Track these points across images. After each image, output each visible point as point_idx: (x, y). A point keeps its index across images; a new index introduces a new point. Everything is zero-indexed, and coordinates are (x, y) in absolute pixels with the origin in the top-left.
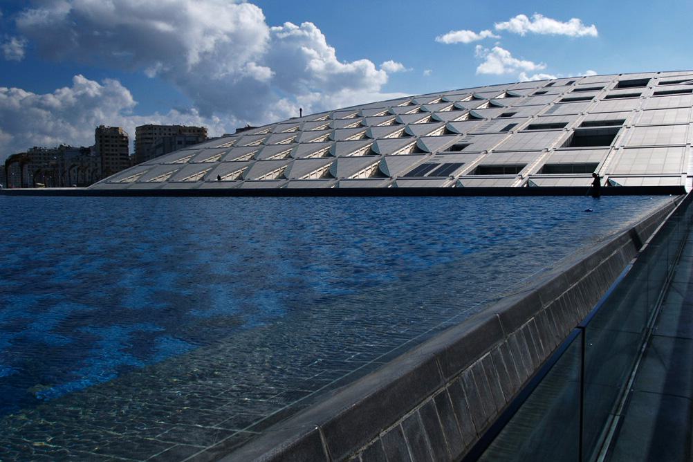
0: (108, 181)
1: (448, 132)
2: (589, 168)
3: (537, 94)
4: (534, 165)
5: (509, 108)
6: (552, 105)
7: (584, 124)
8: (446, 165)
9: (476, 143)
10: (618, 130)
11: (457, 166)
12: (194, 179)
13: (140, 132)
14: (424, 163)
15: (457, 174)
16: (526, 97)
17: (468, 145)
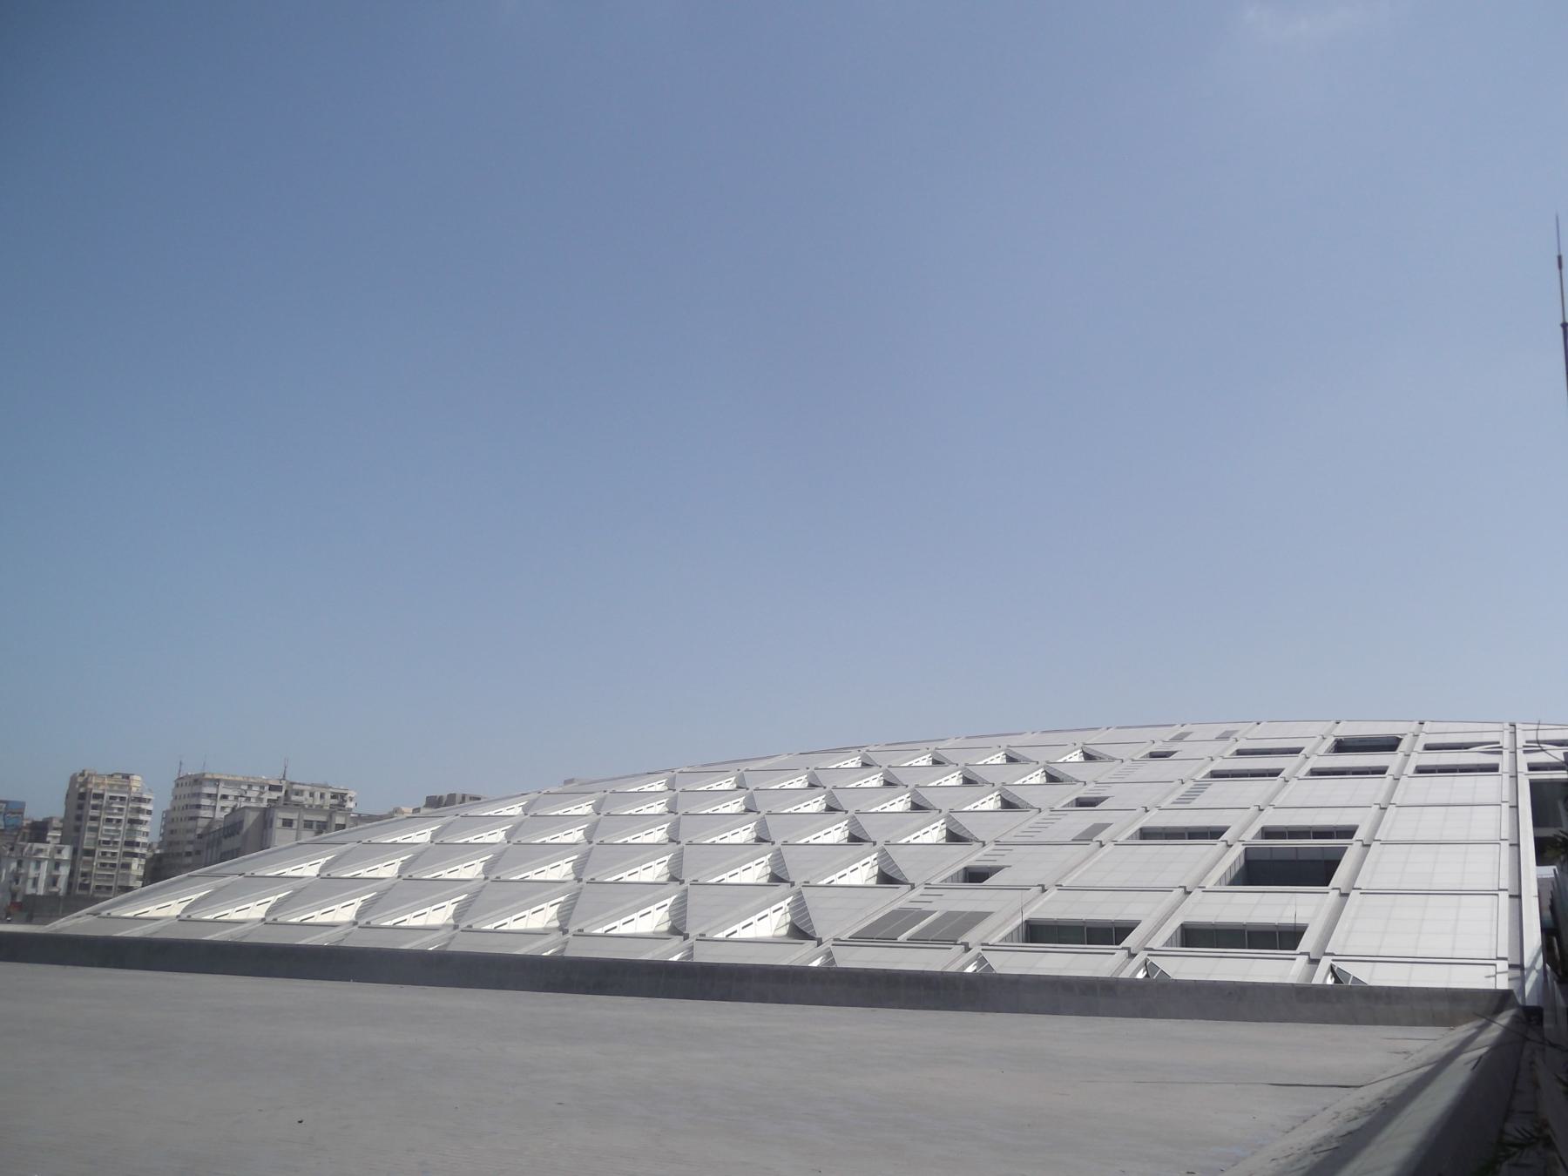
0: (104, 913)
1: (954, 837)
2: (1285, 938)
3: (1153, 755)
4: (1154, 921)
5: (1091, 786)
7: (1267, 833)
8: (949, 916)
9: (1021, 867)
10: (1343, 850)
11: (976, 918)
13: (187, 790)
14: (895, 907)
15: (971, 937)
17: (998, 869)
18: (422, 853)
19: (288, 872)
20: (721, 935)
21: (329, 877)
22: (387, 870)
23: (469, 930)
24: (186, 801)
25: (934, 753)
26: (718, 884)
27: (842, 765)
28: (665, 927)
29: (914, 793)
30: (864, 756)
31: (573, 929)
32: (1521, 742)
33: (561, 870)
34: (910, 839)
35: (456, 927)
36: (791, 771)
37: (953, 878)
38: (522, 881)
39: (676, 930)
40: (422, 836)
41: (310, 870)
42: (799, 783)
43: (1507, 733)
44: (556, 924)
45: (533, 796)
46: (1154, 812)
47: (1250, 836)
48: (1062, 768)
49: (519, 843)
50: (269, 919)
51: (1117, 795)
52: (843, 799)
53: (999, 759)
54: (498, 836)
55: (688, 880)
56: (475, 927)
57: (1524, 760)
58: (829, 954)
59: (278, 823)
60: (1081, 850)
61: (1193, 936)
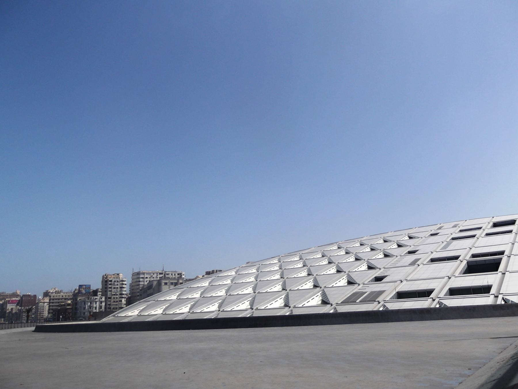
1: (370, 268)
2: (486, 290)
3: (432, 235)
4: (440, 288)
6: (445, 243)
7: (474, 256)
8: (372, 293)
9: (393, 275)
10: (501, 259)
11: (381, 293)
12: (183, 311)
13: (136, 277)
14: (354, 291)
15: (380, 299)
17: (386, 276)
18: (206, 289)
19: (168, 298)
20: (301, 306)
21: (180, 299)
23: (223, 311)
24: (135, 280)
26: (298, 290)
28: (283, 305)
29: (356, 255)
31: (255, 308)
33: (249, 290)
34: (356, 269)
35: (219, 311)
37: (372, 281)
39: (286, 305)
41: (174, 297)
42: (319, 256)
44: (250, 307)
45: (238, 268)
47: (468, 258)
48: (402, 242)
49: (235, 283)
50: (164, 313)
51: (422, 249)
52: (333, 259)
53: (382, 241)
54: (229, 282)
55: (288, 290)
58: (335, 308)
59: (163, 284)
60: (412, 268)
61: (454, 292)
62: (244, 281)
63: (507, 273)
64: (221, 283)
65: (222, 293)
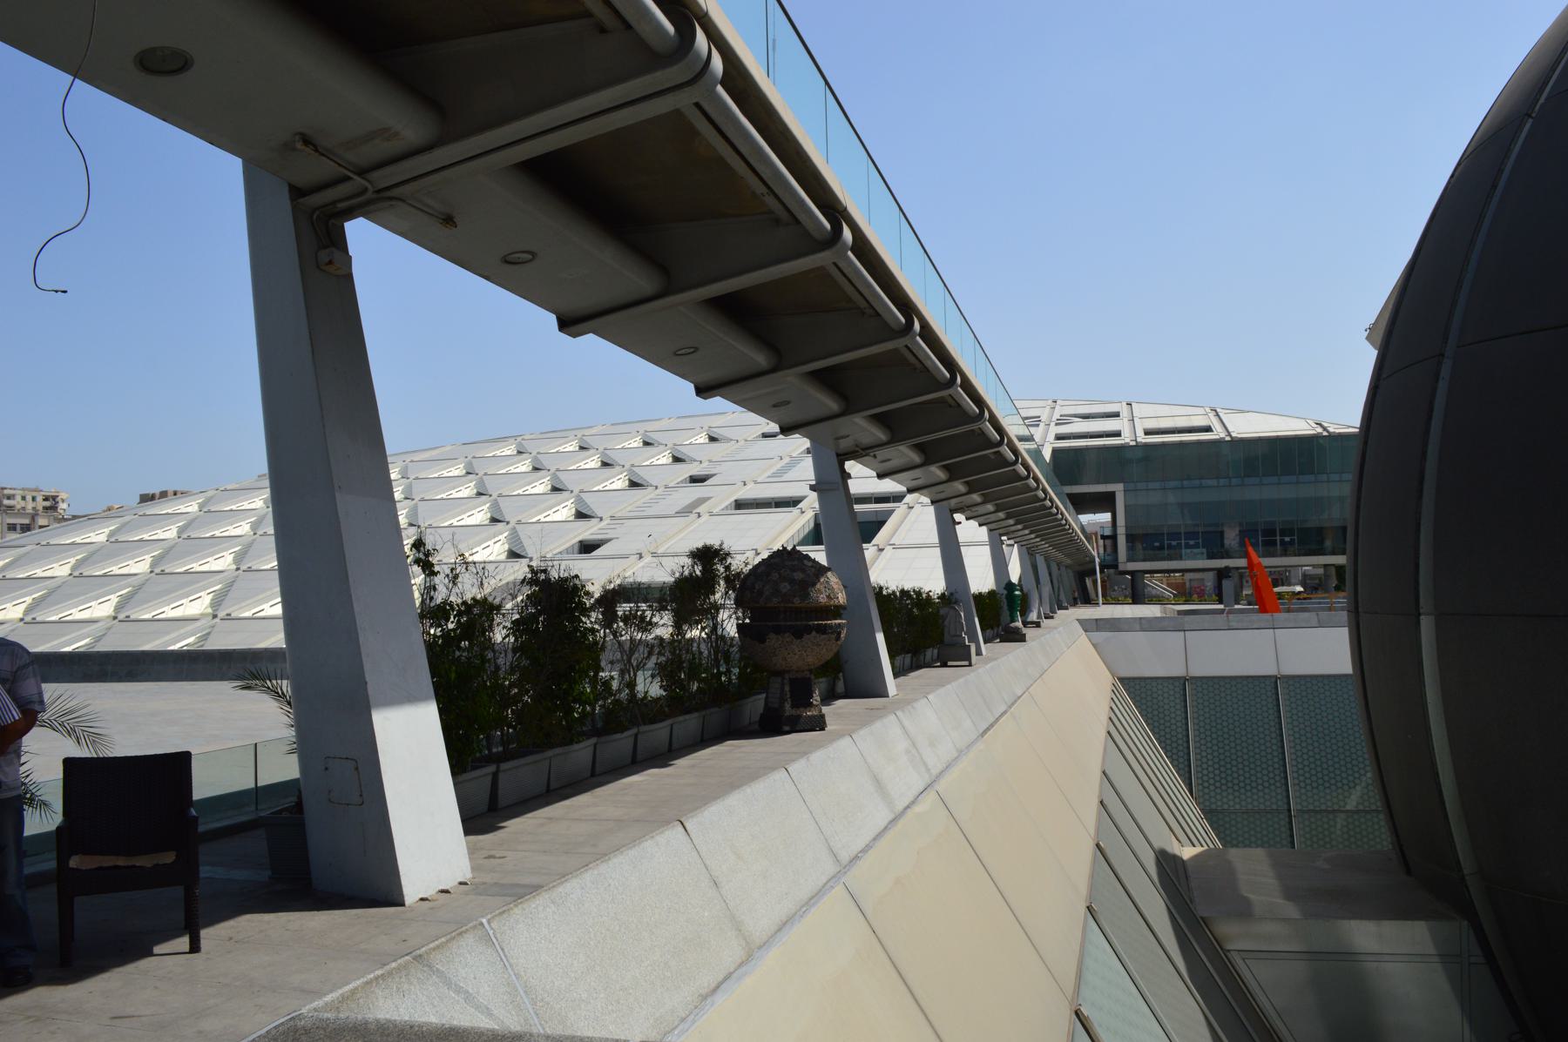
1: (580, 515)
5: (705, 464)
6: (786, 460)
10: (890, 512)
16: (742, 443)
22: (61, 570)
23: (127, 619)
25: (581, 440)
27: (498, 453)
29: (555, 477)
30: (520, 444)
31: (222, 614)
32: (1056, 416)
33: (223, 562)
34: (541, 517)
36: (451, 459)
37: (567, 551)
38: (186, 572)
40: (99, 536)
42: (457, 470)
43: (1048, 410)
44: (210, 610)
45: (210, 494)
46: (750, 485)
49: (189, 538)
51: (724, 473)
52: (491, 486)
53: (636, 442)
54: (170, 533)
56: (133, 617)
57: (1056, 430)
62: (217, 533)
63: (888, 548)
64: (146, 537)
65: (139, 566)
